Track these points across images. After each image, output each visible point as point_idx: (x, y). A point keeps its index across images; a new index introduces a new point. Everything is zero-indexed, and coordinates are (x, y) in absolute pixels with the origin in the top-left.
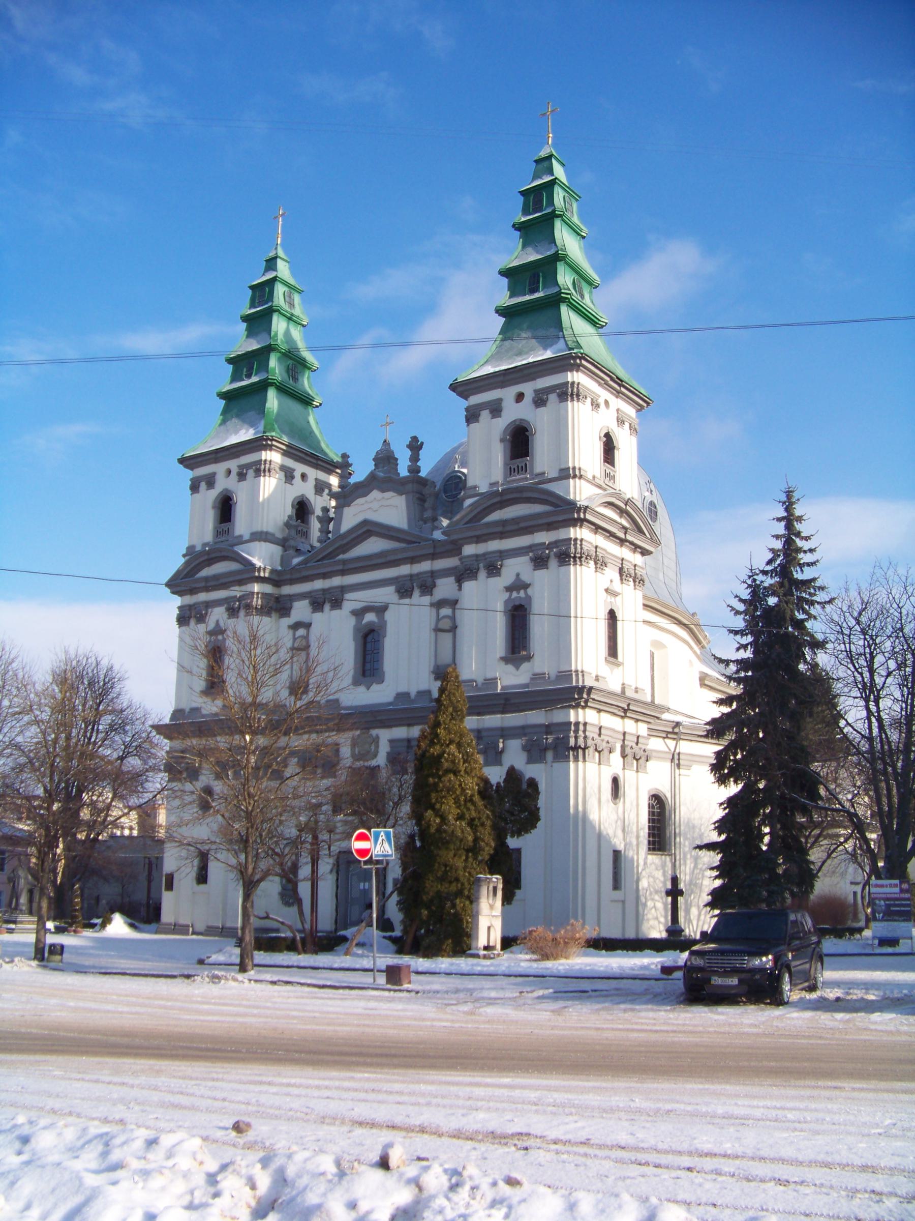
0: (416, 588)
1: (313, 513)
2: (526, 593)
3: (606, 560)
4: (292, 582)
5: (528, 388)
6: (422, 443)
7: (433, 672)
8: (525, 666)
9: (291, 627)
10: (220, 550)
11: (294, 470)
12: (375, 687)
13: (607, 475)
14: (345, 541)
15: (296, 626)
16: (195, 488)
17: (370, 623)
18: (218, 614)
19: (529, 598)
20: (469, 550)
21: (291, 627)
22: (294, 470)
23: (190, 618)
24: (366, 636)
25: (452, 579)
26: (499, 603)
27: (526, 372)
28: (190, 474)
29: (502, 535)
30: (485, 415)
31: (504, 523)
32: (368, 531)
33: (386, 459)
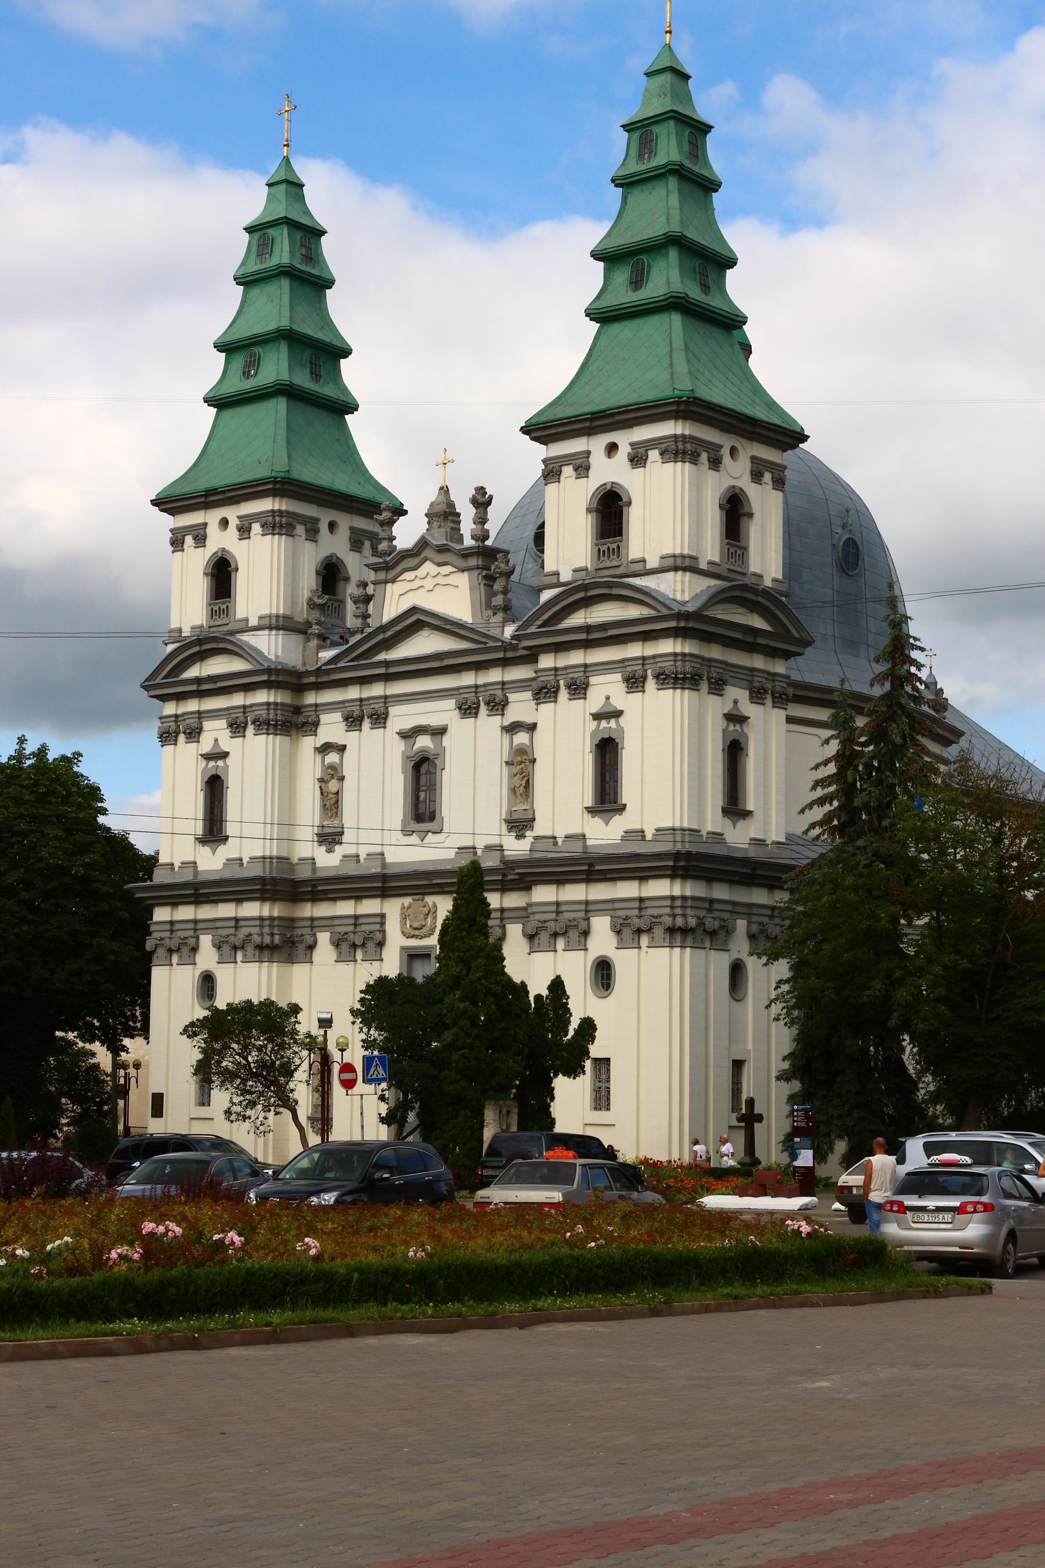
0: (482, 704)
1: (347, 579)
2: (617, 722)
3: (726, 677)
4: (319, 687)
5: (625, 439)
6: (491, 497)
7: (508, 821)
10: (215, 639)
12: (431, 838)
14: (389, 634)
16: (177, 542)
18: (215, 732)
19: (621, 730)
20: (546, 661)
21: (316, 749)
22: (318, 520)
23: (177, 733)
25: (528, 695)
27: (618, 418)
28: (168, 522)
29: (588, 644)
30: (568, 471)
31: (588, 628)
32: (419, 621)
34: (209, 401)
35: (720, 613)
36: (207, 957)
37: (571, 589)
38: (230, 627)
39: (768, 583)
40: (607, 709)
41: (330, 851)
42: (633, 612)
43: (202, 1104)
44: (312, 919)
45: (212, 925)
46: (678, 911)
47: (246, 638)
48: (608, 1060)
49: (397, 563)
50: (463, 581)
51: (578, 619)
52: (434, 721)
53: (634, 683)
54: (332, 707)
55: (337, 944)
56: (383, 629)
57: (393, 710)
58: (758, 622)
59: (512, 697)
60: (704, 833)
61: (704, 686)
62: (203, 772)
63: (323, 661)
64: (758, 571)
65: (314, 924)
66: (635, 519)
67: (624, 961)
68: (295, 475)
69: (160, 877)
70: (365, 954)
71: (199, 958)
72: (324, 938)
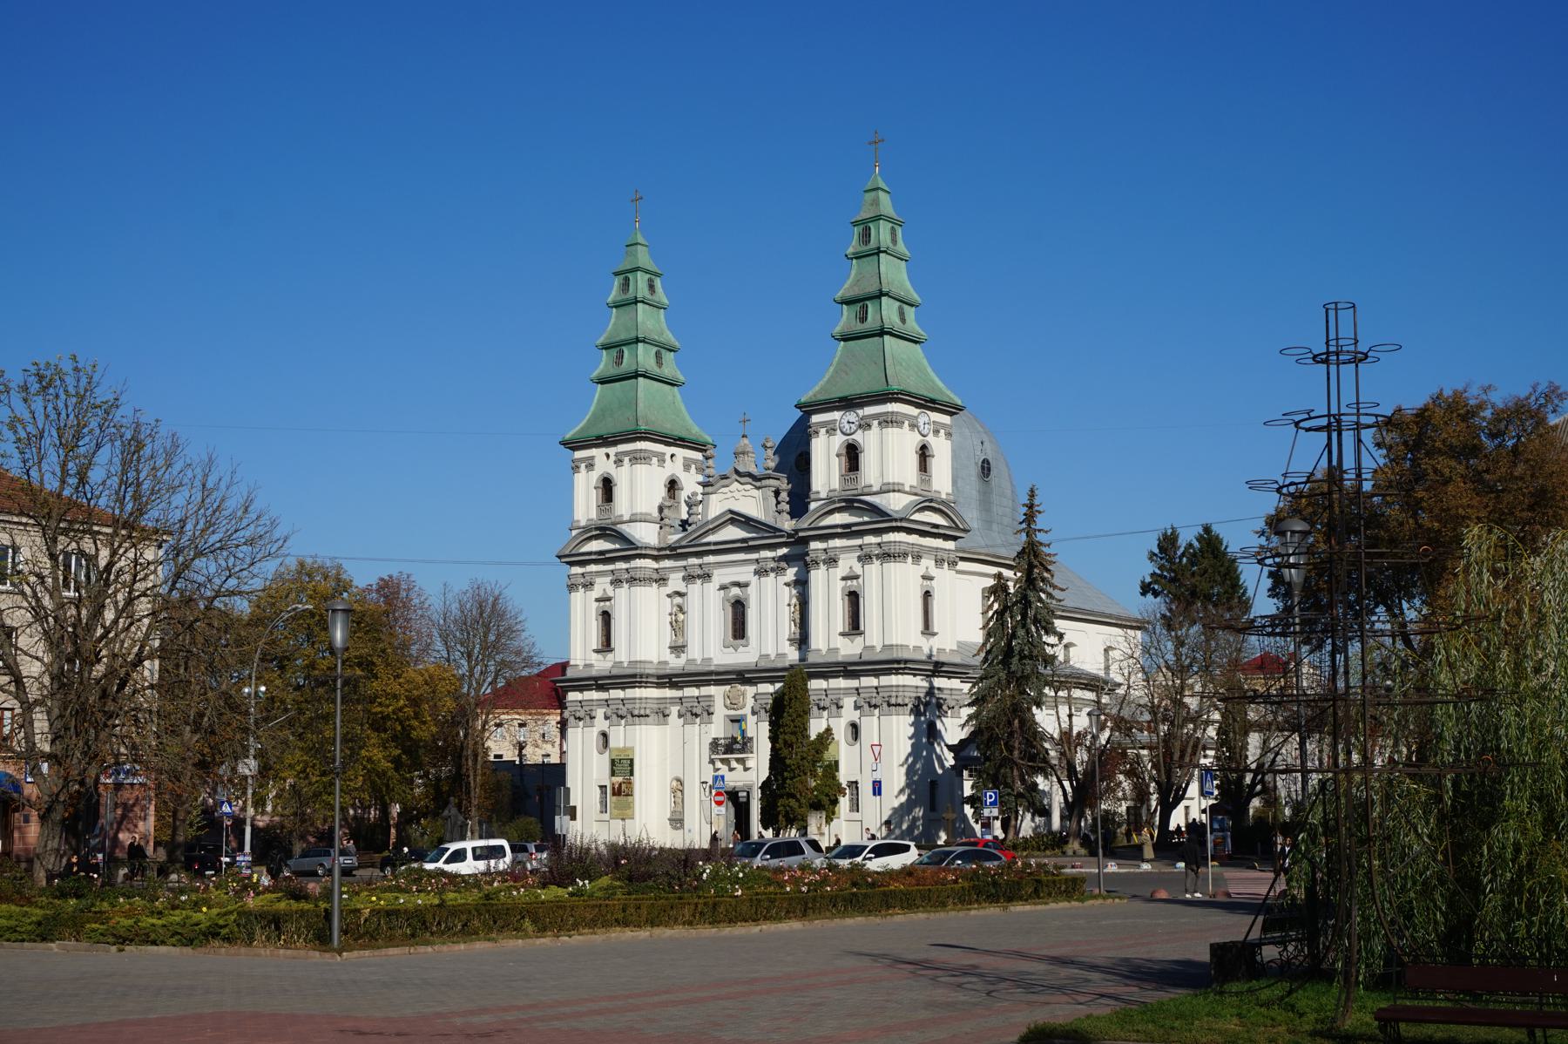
8: (859, 639)
9: (669, 596)
11: (664, 454)
12: (741, 649)
13: (922, 481)
18: (602, 585)
20: (814, 545)
21: (669, 596)
22: (664, 454)
26: (839, 587)
35: (916, 517)
36: (601, 723)
37: (830, 501)
38: (613, 520)
39: (944, 496)
40: (852, 574)
41: (678, 657)
46: (901, 694)
48: (856, 782)
49: (717, 482)
50: (756, 493)
52: (742, 579)
56: (707, 523)
57: (716, 572)
60: (911, 647)
61: (910, 559)
62: (597, 609)
63: (670, 542)
64: (937, 489)
66: (869, 461)
69: (570, 673)
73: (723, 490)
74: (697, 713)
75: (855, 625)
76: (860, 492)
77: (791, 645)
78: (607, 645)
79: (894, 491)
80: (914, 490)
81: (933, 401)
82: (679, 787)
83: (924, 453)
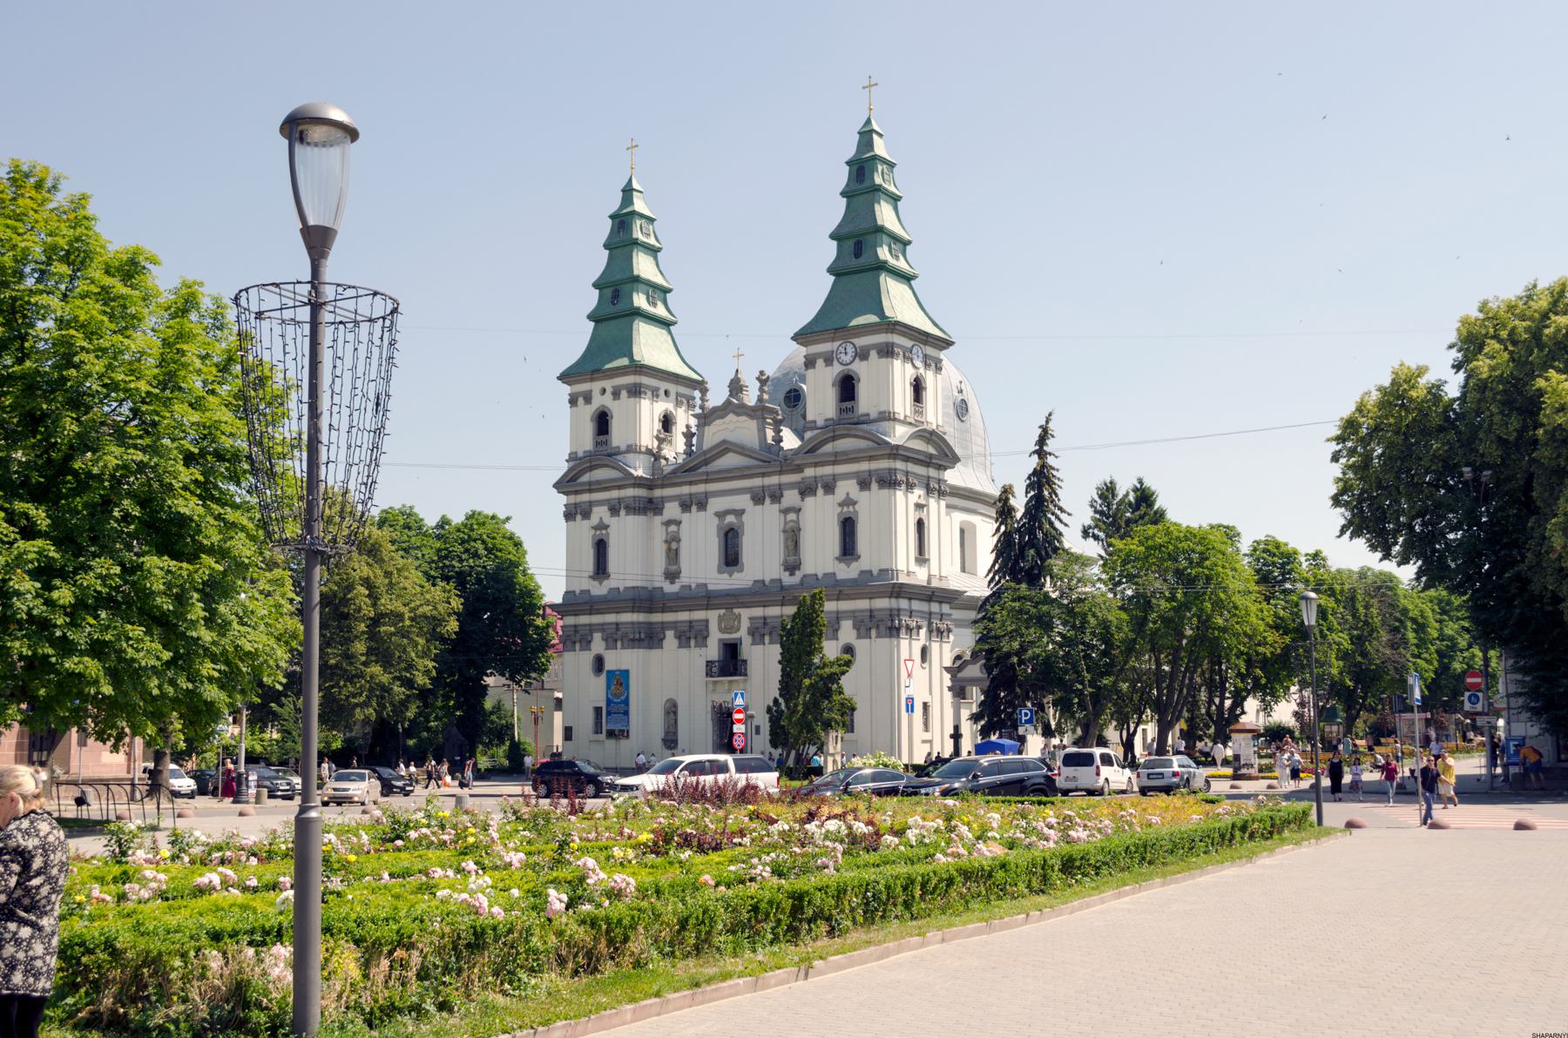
4: (663, 486)
8: (854, 565)
12: (736, 575)
13: (916, 412)
15: (668, 523)
16: (573, 401)
17: (731, 523)
18: (600, 513)
19: (856, 512)
20: (809, 472)
24: (726, 534)
25: (796, 492)
28: (565, 390)
29: (834, 463)
30: (820, 363)
31: (836, 454)
33: (736, 387)
34: (590, 317)
36: (598, 645)
42: (863, 444)
43: (596, 732)
44: (662, 623)
45: (601, 627)
47: (619, 457)
51: (828, 448)
52: (738, 507)
53: (864, 485)
54: (671, 498)
55: (679, 637)
56: (705, 453)
58: (932, 450)
59: (787, 493)
61: (903, 487)
65: (664, 626)
67: (861, 646)
68: (646, 363)
70: (696, 642)
71: (593, 645)
72: (670, 634)
73: (718, 422)
74: (692, 635)
75: (848, 549)
76: (856, 420)
77: (786, 570)
78: (601, 570)
79: (890, 419)
80: (908, 420)
81: (927, 335)
82: (672, 710)
83: (918, 387)
